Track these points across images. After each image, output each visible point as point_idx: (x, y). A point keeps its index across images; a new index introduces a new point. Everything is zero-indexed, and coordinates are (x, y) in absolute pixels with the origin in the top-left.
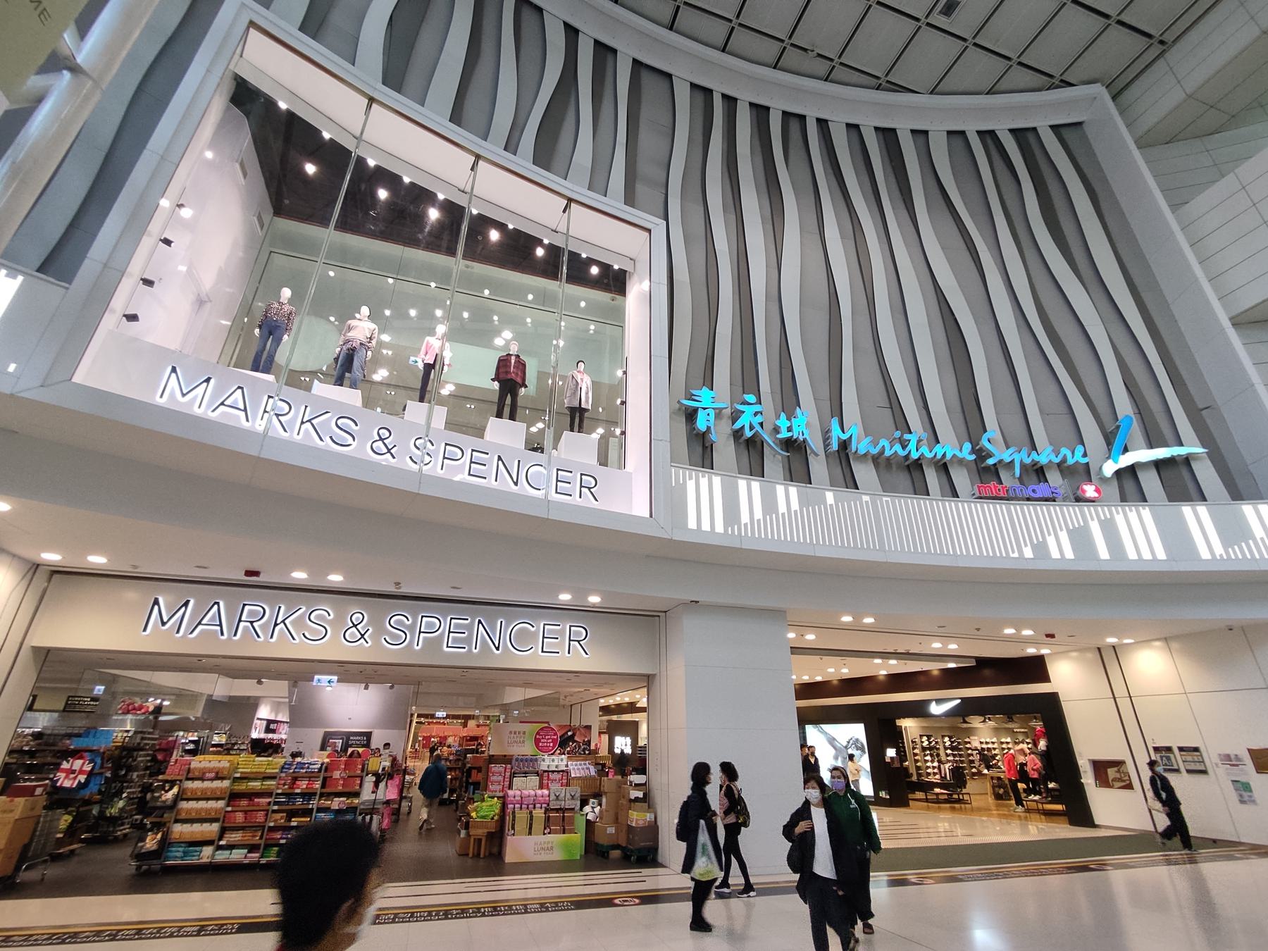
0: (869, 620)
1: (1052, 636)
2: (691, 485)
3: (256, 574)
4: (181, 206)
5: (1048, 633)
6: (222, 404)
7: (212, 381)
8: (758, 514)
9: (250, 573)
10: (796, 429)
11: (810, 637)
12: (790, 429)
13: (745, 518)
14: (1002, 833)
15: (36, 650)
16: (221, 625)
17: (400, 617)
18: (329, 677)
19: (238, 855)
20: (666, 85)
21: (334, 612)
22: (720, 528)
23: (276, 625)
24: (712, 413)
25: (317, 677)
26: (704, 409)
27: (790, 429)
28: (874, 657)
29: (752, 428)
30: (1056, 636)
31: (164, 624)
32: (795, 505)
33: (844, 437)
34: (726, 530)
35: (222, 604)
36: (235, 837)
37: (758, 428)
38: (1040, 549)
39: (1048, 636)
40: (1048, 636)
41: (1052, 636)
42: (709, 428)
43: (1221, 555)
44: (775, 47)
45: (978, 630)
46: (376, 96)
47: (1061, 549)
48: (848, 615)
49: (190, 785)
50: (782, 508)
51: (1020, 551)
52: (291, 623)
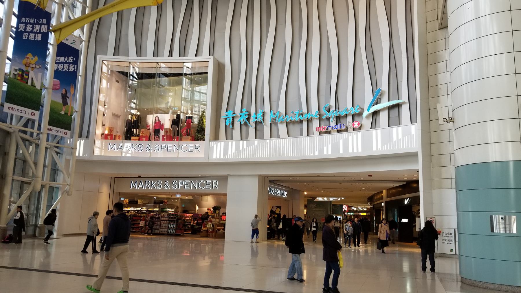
2: (215, 146)
3: (140, 176)
4: (105, 105)
6: (118, 148)
7: (116, 144)
8: (233, 151)
9: (139, 176)
12: (256, 118)
13: (229, 153)
15: (117, 193)
16: (142, 186)
17: (175, 182)
18: (179, 195)
21: (162, 181)
22: (222, 157)
23: (152, 185)
24: (231, 119)
25: (176, 195)
26: (228, 118)
27: (256, 118)
29: (243, 120)
31: (133, 186)
32: (245, 147)
33: (274, 117)
34: (224, 157)
35: (142, 181)
37: (246, 120)
39: (369, 176)
42: (229, 124)
46: (129, 61)
50: (241, 148)
51: (314, 153)
52: (154, 184)
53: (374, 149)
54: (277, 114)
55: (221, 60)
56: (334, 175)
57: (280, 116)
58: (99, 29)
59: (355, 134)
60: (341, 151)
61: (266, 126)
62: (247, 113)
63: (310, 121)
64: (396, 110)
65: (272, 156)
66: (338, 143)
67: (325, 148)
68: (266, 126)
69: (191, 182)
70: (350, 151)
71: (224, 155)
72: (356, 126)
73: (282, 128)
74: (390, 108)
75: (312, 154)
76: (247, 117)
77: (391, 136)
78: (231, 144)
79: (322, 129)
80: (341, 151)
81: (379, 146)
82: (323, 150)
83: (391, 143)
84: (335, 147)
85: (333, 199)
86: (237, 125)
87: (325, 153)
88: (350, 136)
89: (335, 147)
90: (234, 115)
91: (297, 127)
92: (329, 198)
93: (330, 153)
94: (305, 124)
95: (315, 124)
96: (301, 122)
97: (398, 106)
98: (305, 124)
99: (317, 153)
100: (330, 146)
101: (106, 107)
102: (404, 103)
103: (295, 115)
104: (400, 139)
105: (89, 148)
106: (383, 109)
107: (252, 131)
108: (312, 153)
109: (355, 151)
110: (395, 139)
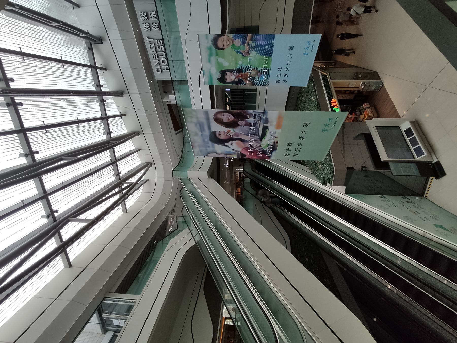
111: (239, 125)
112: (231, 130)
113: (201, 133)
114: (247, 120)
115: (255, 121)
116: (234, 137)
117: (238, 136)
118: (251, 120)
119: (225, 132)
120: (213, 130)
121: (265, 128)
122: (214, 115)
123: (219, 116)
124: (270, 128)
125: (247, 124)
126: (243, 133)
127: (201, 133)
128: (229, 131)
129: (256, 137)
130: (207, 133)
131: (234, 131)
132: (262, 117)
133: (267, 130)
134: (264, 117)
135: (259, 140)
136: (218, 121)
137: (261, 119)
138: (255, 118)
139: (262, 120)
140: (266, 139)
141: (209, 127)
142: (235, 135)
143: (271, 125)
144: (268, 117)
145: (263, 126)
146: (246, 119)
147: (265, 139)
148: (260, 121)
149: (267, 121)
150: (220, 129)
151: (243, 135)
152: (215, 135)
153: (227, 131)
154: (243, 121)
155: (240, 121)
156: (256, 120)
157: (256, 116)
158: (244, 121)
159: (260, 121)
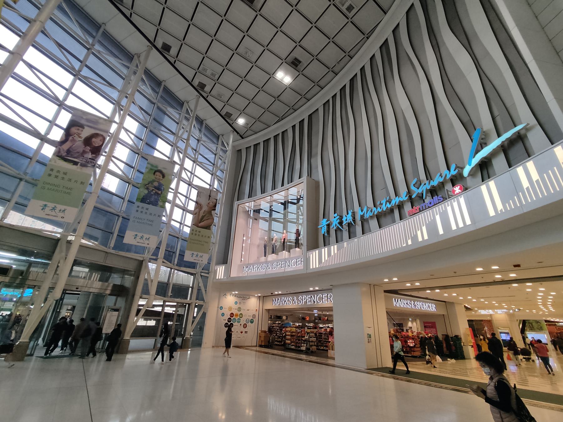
0: (395, 279)
1: (518, 266)
5: (515, 264)
8: (326, 259)
9: (271, 294)
10: (348, 220)
11: (417, 284)
13: (323, 261)
14: (425, 369)
15: (266, 310)
19: (293, 347)
20: (313, 116)
22: (317, 266)
24: (326, 226)
27: (346, 220)
28: (511, 283)
29: (336, 225)
30: (521, 266)
33: (362, 214)
34: (319, 266)
36: (293, 344)
37: (338, 225)
38: (414, 238)
39: (515, 266)
40: (515, 266)
41: (518, 266)
42: (325, 232)
43: (501, 210)
44: (331, 73)
45: (455, 273)
47: (423, 235)
48: (396, 278)
49: (287, 333)
51: (407, 243)
53: (492, 213)
54: (365, 210)
55: (316, 179)
56: (455, 273)
57: (367, 211)
58: (241, 187)
59: (454, 201)
60: (441, 232)
61: (358, 225)
62: (338, 217)
63: (400, 207)
64: (520, 145)
65: (362, 256)
66: (434, 221)
67: (419, 233)
68: (358, 225)
69: (311, 297)
70: (454, 227)
71: (319, 264)
72: (458, 192)
73: (374, 223)
74: (505, 149)
75: (405, 245)
76: (338, 221)
77: (516, 182)
78: (325, 251)
79: (415, 211)
80: (441, 232)
81: (500, 206)
82: (416, 236)
83: (520, 193)
84: (432, 229)
85: (502, 312)
86: (333, 233)
87: (420, 239)
88: (448, 206)
89: (432, 229)
90: (328, 222)
91: (389, 218)
92: (496, 310)
93: (426, 237)
94: (396, 212)
95: (407, 207)
96: (391, 210)
97: (520, 138)
98: (396, 212)
99: (410, 242)
100: (424, 229)
101: (244, 238)
102: (527, 129)
103: (382, 204)
104: (537, 181)
105: (228, 272)
106: (494, 154)
107: (346, 234)
108: (404, 244)
109: (461, 225)
110: (525, 184)
111: (85, 146)
112: (83, 139)
113: (85, 117)
114: (90, 153)
115: (87, 158)
116: (71, 138)
117: (71, 141)
118: (90, 156)
119: (81, 134)
120: (86, 127)
121: (75, 163)
122: (102, 136)
123: (101, 138)
124: (75, 167)
125: (84, 152)
126: (74, 146)
127: (85, 117)
128: (80, 137)
129: (64, 154)
130: (83, 122)
131: (79, 141)
132: (91, 164)
133: (72, 164)
134: (89, 165)
135: (60, 154)
136: (96, 135)
137: (88, 162)
138: (90, 159)
139: (86, 163)
140: (59, 160)
141: (88, 126)
142: (74, 141)
143: (78, 168)
144: (89, 168)
145: (79, 162)
146: (91, 153)
147: (60, 159)
148: (86, 162)
149: (83, 165)
150: (86, 132)
151: (71, 145)
152: (79, 126)
153: (80, 136)
154: (90, 151)
155: (90, 148)
156: (88, 159)
157: (92, 160)
158: (89, 151)
159: (86, 162)
